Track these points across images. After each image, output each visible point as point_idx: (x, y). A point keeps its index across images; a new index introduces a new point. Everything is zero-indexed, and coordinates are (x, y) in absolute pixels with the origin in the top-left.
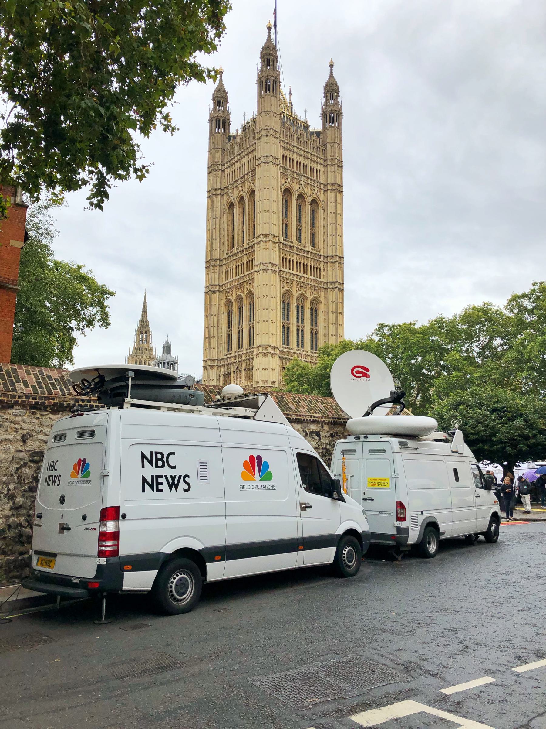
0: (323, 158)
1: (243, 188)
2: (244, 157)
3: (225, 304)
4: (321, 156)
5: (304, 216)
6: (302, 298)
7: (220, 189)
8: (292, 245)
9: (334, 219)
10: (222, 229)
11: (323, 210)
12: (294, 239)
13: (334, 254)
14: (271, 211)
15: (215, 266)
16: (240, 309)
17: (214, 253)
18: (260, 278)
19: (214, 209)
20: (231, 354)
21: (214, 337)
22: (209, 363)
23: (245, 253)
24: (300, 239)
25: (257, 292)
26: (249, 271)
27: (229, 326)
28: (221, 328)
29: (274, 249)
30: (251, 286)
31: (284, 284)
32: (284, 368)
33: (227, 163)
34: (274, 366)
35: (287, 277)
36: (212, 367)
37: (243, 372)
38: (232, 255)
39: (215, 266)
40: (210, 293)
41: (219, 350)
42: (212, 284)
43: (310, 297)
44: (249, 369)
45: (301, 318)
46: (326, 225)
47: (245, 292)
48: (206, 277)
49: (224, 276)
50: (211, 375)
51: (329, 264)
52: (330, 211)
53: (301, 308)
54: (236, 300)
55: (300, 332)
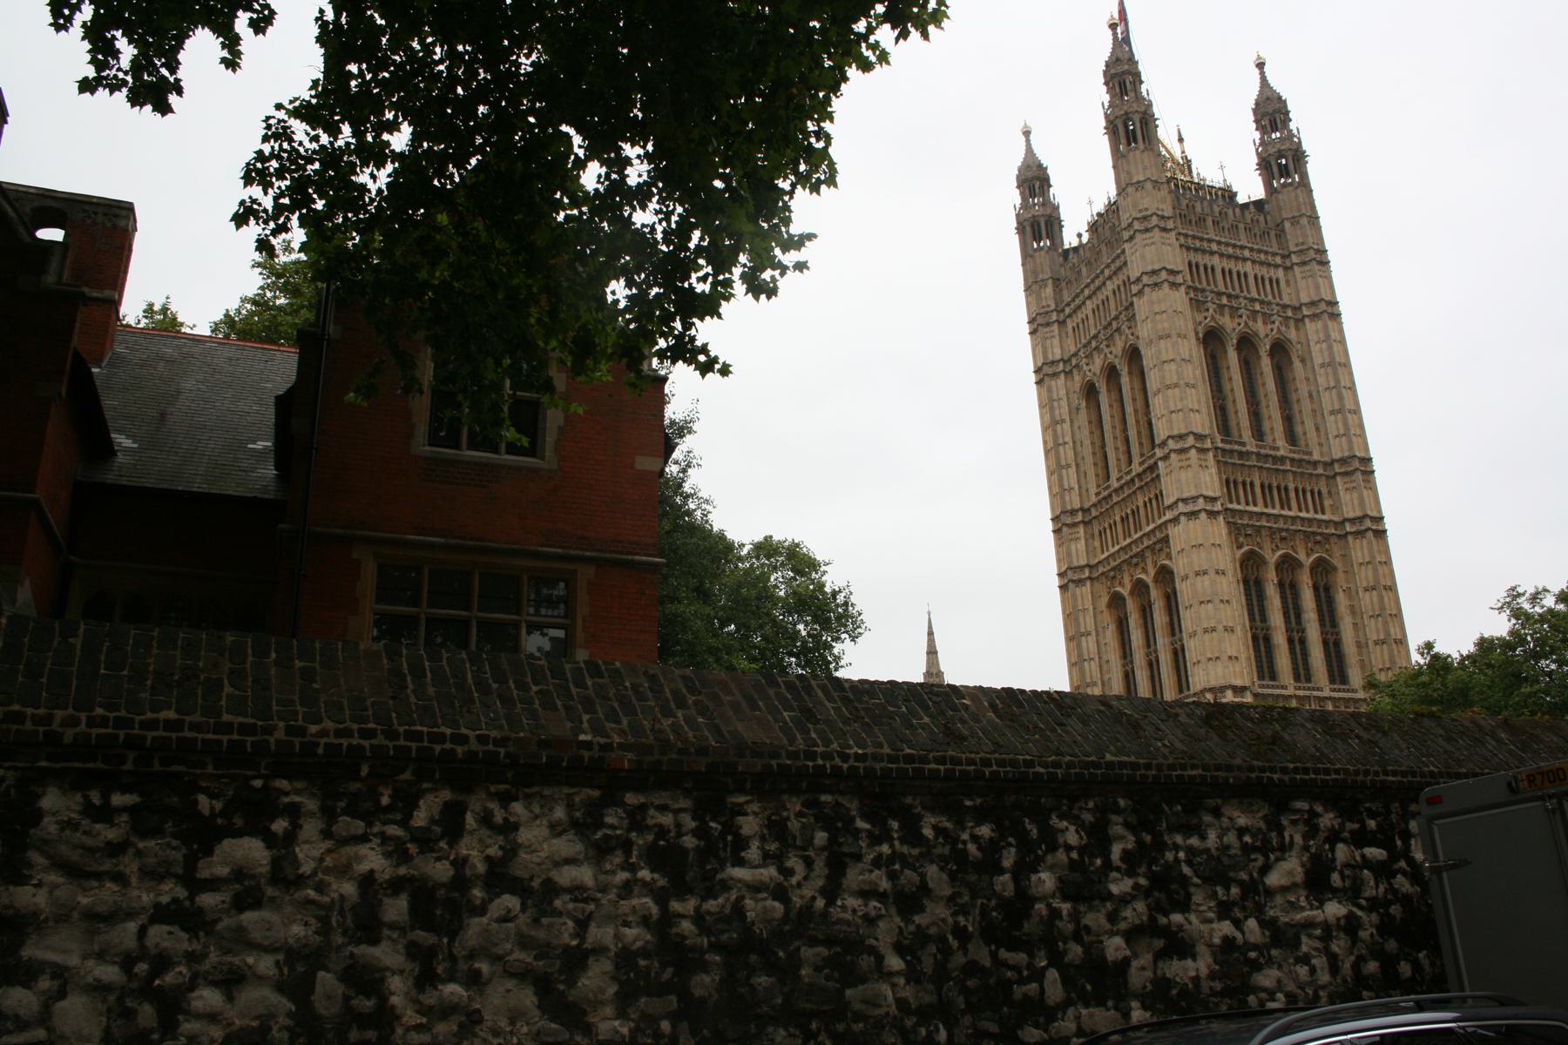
0: (1281, 252)
2: (1104, 284)
3: (1109, 605)
6: (1288, 565)
7: (1062, 359)
8: (1244, 449)
9: (1331, 378)
11: (1303, 361)
12: (1247, 435)
13: (1346, 454)
14: (1182, 382)
15: (1074, 525)
16: (1146, 612)
17: (1067, 498)
18: (1180, 535)
19: (1055, 404)
23: (1137, 485)
24: (1258, 434)
25: (1179, 566)
26: (1153, 521)
27: (1124, 653)
28: (1108, 661)
29: (1204, 464)
30: (1163, 555)
31: (1241, 539)
33: (1068, 305)
35: (1245, 522)
39: (1074, 525)
40: (1071, 586)
43: (1307, 560)
45: (1293, 612)
46: (1314, 394)
47: (1152, 572)
48: (1058, 553)
49: (1097, 544)
51: (1339, 479)
52: (1318, 361)
53: (1289, 590)
54: (1132, 593)
55: (1298, 644)
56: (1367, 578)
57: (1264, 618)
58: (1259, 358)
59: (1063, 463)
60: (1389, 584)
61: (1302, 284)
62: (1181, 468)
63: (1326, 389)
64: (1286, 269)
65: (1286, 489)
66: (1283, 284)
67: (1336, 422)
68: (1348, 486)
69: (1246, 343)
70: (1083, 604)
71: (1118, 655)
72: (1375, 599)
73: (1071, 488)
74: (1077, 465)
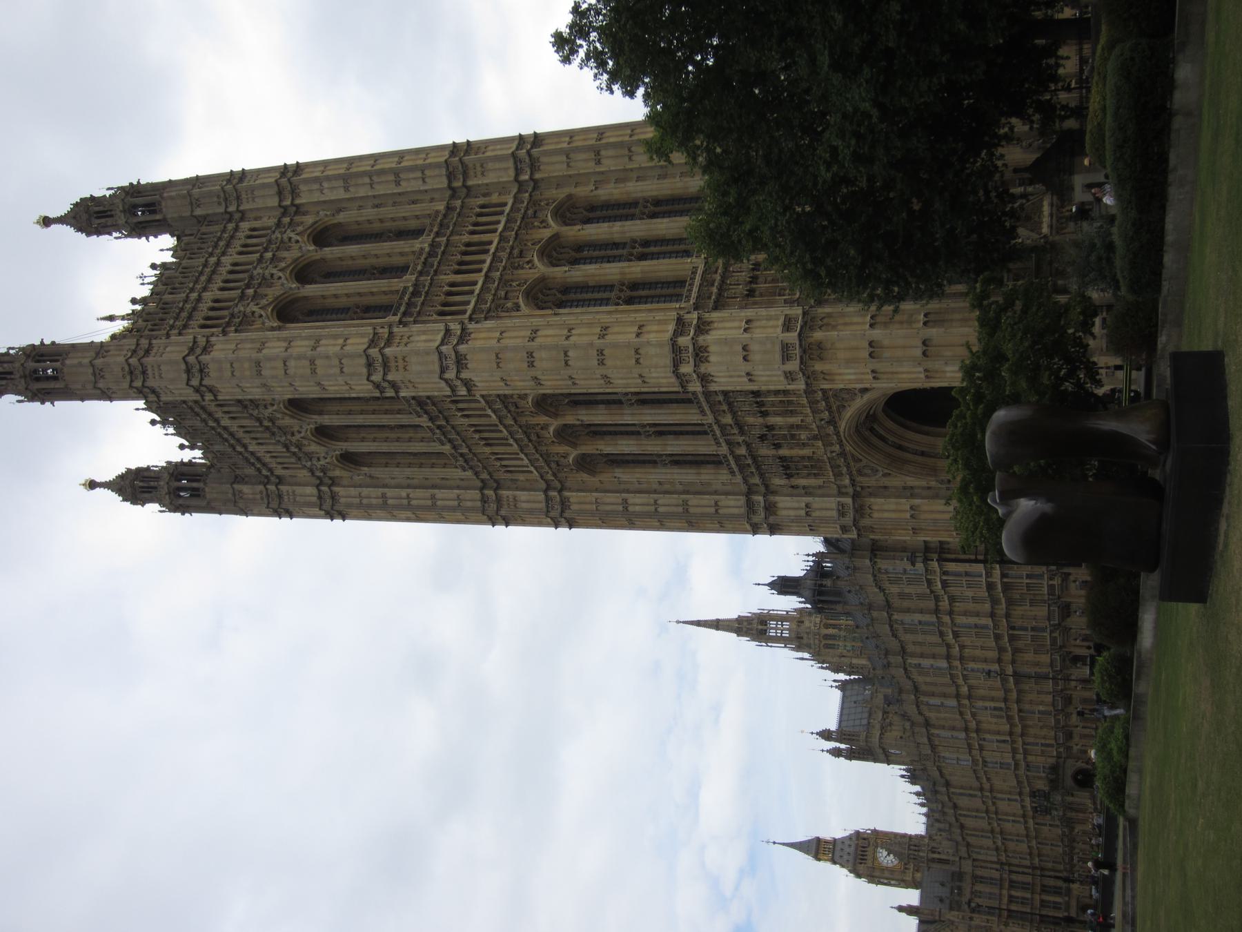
1: (296, 429)
3: (592, 472)
4: (217, 228)
5: (350, 262)
6: (553, 251)
7: (317, 486)
8: (411, 289)
9: (360, 181)
10: (409, 481)
11: (339, 210)
12: (397, 284)
13: (444, 171)
16: (597, 432)
17: (469, 504)
18: (484, 377)
19: (365, 501)
20: (725, 456)
21: (685, 503)
22: (759, 517)
23: (444, 423)
27: (649, 462)
28: (660, 483)
29: (405, 340)
30: (522, 403)
32: (751, 293)
34: (736, 324)
36: (770, 508)
37: (773, 420)
39: (499, 500)
40: (566, 515)
42: (545, 509)
44: (760, 404)
46: (377, 201)
47: (543, 419)
49: (521, 477)
50: (792, 513)
52: (341, 194)
53: (581, 253)
54: (574, 445)
56: (586, 160)
57: (609, 287)
58: (323, 260)
59: (429, 503)
60: (596, 135)
61: (260, 203)
62: (405, 369)
63: (372, 187)
64: (242, 219)
65: (468, 245)
66: (257, 224)
67: (408, 180)
68: (479, 174)
69: (303, 274)
70: (591, 503)
72: (611, 153)
74: (434, 487)
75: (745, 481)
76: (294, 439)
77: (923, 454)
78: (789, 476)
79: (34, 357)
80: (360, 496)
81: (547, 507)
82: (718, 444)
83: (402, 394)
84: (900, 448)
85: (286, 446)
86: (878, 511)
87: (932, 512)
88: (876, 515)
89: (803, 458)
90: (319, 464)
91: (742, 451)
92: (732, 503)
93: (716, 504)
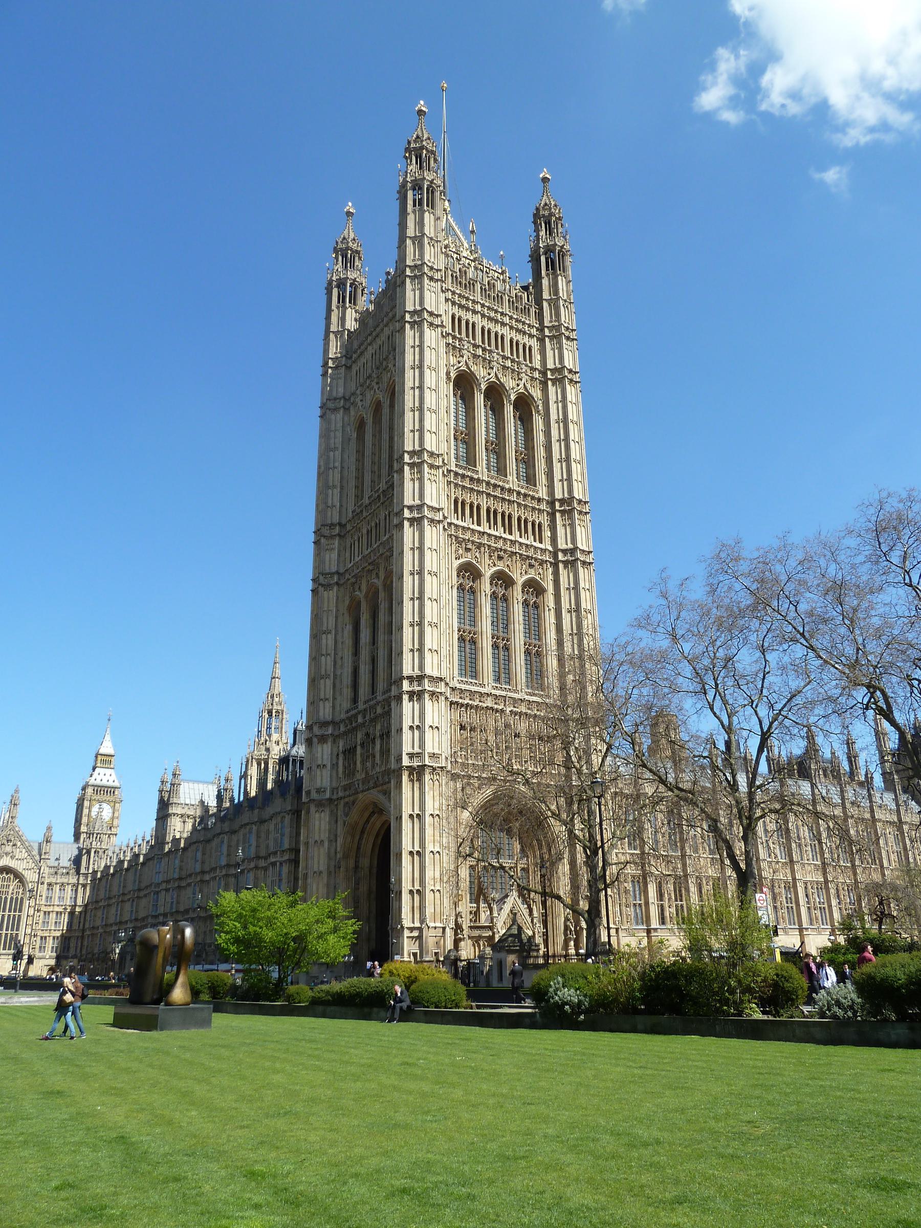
3: (349, 608)
8: (476, 477)
10: (346, 468)
19: (332, 434)
21: (328, 676)
27: (356, 650)
29: (433, 478)
31: (461, 552)
34: (436, 720)
36: (323, 739)
37: (378, 742)
38: (362, 511)
39: (332, 537)
41: (338, 702)
42: (324, 572)
45: (502, 622)
53: (501, 601)
54: (366, 596)
57: (473, 623)
71: (350, 653)
73: (334, 506)
74: (342, 488)
75: (342, 721)
76: (374, 384)
77: (358, 848)
78: (344, 752)
79: (431, 186)
80: (336, 430)
81: (326, 574)
82: (365, 702)
83: (395, 475)
84: (363, 832)
85: (369, 377)
86: (320, 817)
87: (319, 855)
88: (317, 815)
89: (355, 763)
90: (358, 400)
91: (360, 720)
92: (327, 710)
93: (327, 699)
